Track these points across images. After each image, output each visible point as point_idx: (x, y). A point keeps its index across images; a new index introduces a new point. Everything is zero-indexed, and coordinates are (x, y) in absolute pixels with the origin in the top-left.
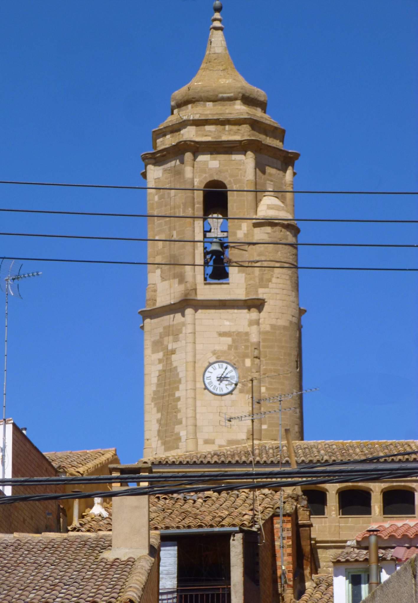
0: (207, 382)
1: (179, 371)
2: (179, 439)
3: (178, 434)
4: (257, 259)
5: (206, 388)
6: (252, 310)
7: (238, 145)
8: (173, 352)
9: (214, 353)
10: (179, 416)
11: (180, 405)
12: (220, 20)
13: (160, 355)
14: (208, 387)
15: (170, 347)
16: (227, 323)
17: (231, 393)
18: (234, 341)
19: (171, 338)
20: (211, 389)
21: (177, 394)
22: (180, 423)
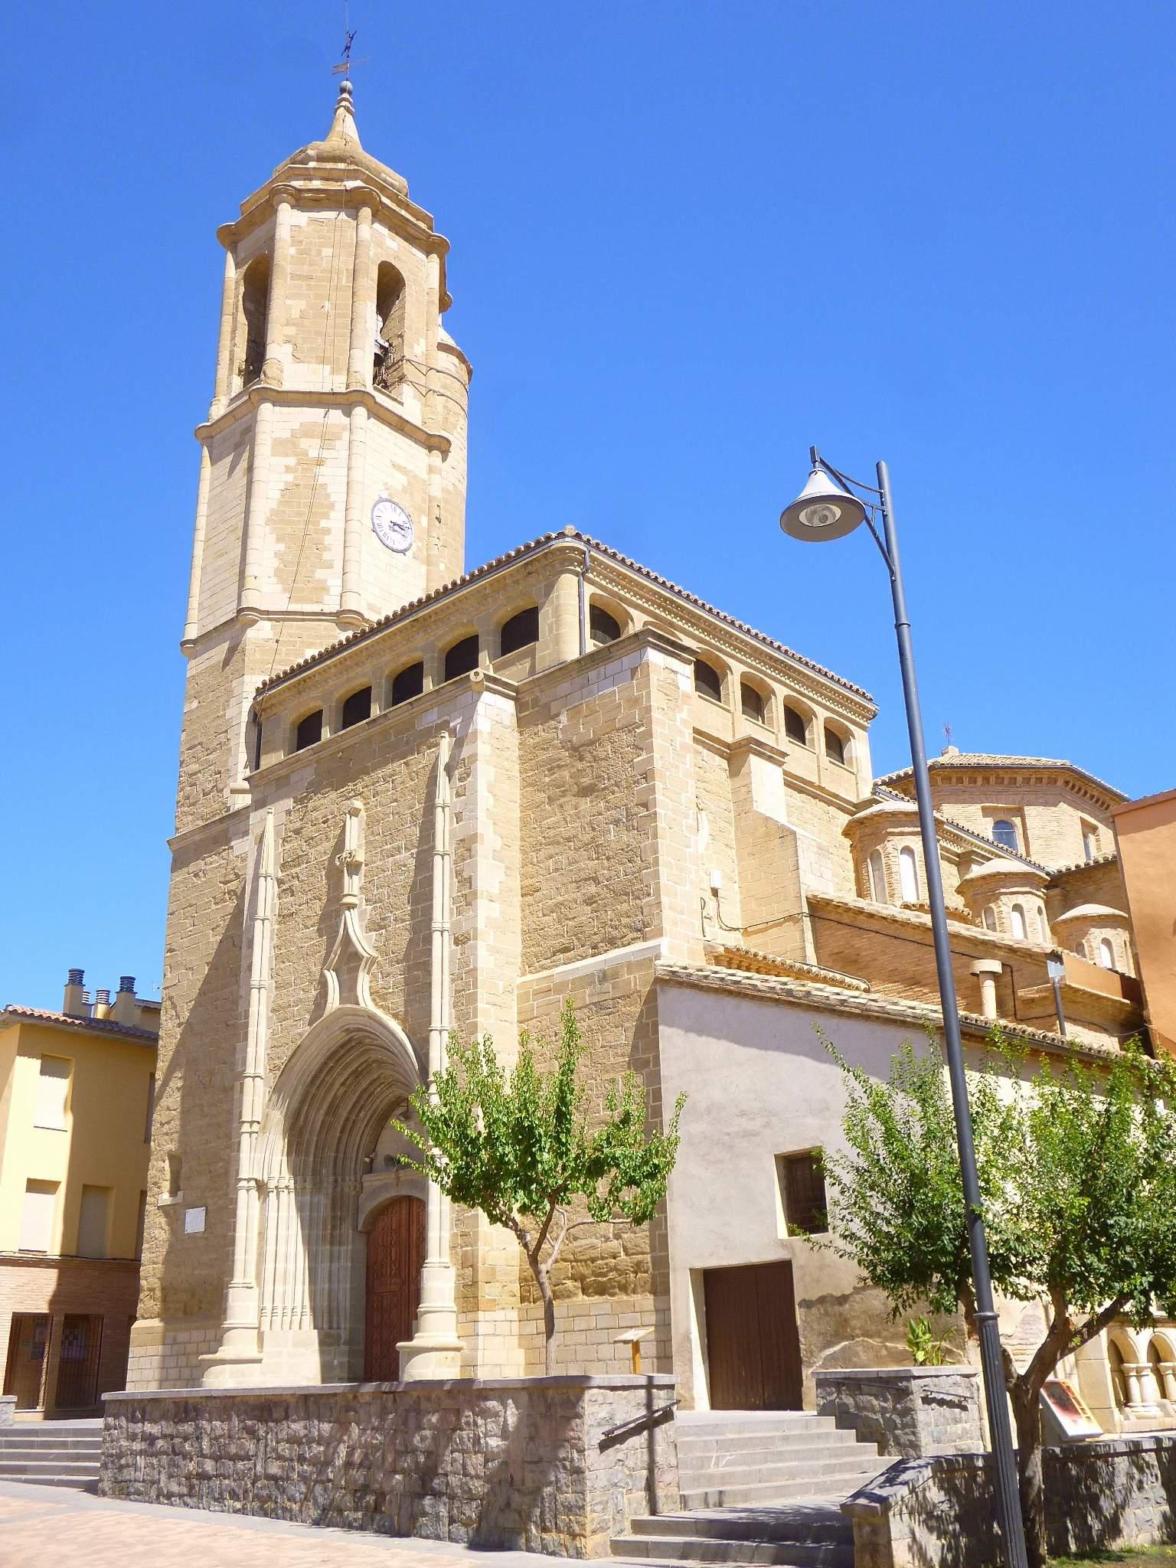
1: (329, 490)
4: (442, 391)
6: (435, 452)
7: (425, 238)
8: (320, 462)
10: (326, 556)
11: (328, 540)
12: (350, 102)
13: (291, 461)
14: (378, 530)
15: (313, 453)
17: (403, 552)
18: (409, 483)
20: (381, 534)
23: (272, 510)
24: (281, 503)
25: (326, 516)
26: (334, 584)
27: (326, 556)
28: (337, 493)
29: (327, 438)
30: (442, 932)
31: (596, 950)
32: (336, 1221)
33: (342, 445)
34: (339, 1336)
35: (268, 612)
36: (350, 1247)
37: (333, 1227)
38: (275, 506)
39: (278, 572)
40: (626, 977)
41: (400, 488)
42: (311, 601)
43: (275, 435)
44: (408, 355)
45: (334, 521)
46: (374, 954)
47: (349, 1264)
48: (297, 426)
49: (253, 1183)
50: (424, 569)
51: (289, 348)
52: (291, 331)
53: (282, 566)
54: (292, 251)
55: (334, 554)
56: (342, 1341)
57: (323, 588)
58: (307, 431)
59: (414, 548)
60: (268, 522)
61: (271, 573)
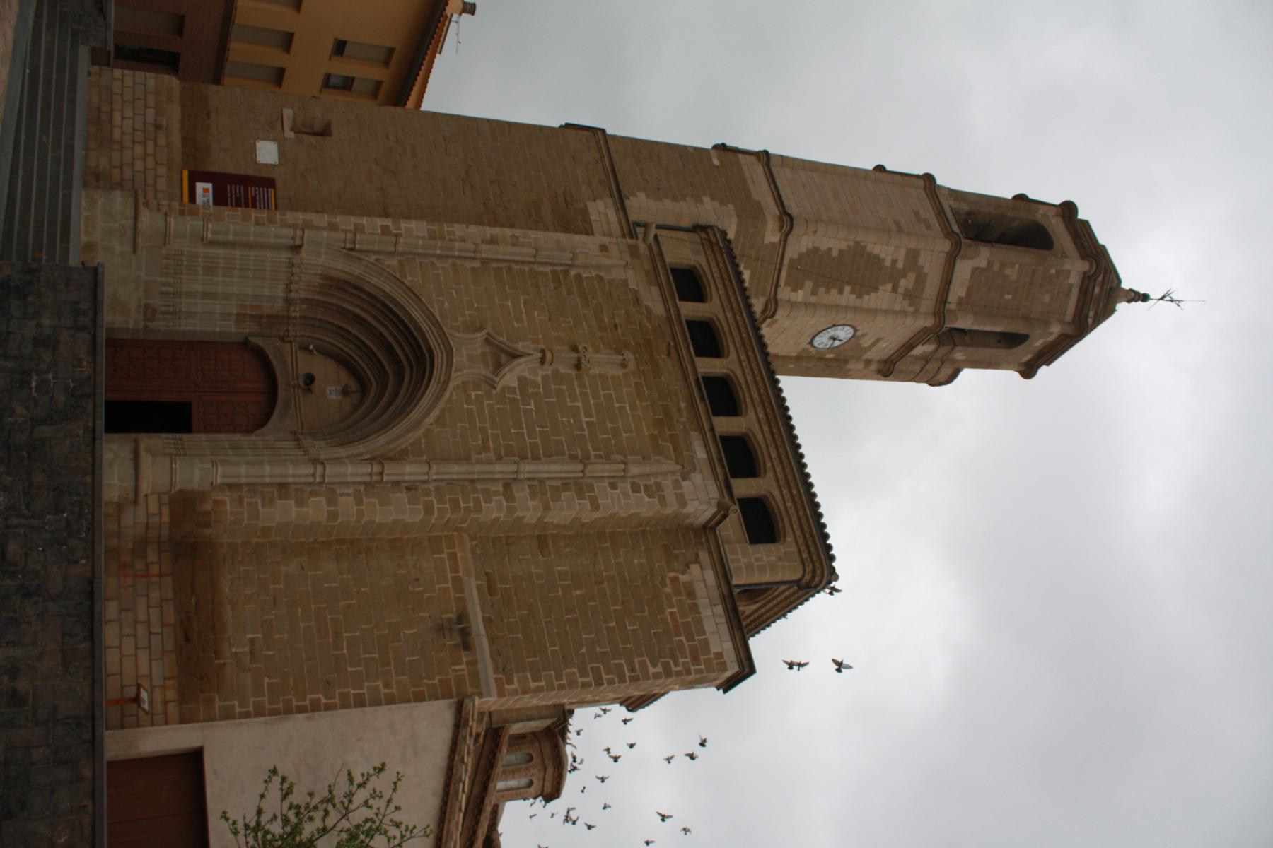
0: (840, 328)
2: (795, 290)
3: (802, 288)
4: (924, 370)
5: (834, 326)
8: (894, 290)
9: (863, 335)
10: (822, 290)
11: (834, 292)
13: (900, 265)
14: (833, 329)
15: (903, 283)
16: (885, 345)
19: (910, 286)
21: (847, 289)
22: (814, 293)
23: (865, 247)
24: (870, 254)
25: (852, 292)
26: (799, 296)
27: (822, 290)
28: (870, 300)
29: (912, 296)
30: (516, 472)
31: (488, 622)
32: (257, 319)
33: (905, 305)
34: (153, 321)
35: (786, 241)
36: (233, 330)
37: (252, 316)
38: (868, 249)
39: (816, 249)
40: (464, 660)
41: (861, 342)
42: (788, 275)
43: (922, 252)
44: (958, 348)
45: (848, 297)
46: (499, 387)
47: (218, 329)
48: (926, 270)
49: (298, 242)
50: (794, 354)
51: (983, 264)
52: (996, 267)
53: (820, 253)
54: (1053, 271)
55: (824, 297)
56: (148, 324)
57: (796, 286)
58: (921, 279)
59: (812, 349)
60: (857, 243)
61: (816, 245)
